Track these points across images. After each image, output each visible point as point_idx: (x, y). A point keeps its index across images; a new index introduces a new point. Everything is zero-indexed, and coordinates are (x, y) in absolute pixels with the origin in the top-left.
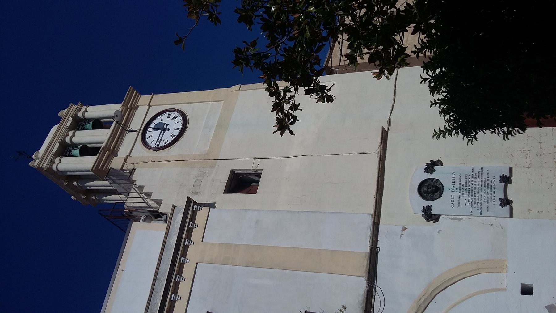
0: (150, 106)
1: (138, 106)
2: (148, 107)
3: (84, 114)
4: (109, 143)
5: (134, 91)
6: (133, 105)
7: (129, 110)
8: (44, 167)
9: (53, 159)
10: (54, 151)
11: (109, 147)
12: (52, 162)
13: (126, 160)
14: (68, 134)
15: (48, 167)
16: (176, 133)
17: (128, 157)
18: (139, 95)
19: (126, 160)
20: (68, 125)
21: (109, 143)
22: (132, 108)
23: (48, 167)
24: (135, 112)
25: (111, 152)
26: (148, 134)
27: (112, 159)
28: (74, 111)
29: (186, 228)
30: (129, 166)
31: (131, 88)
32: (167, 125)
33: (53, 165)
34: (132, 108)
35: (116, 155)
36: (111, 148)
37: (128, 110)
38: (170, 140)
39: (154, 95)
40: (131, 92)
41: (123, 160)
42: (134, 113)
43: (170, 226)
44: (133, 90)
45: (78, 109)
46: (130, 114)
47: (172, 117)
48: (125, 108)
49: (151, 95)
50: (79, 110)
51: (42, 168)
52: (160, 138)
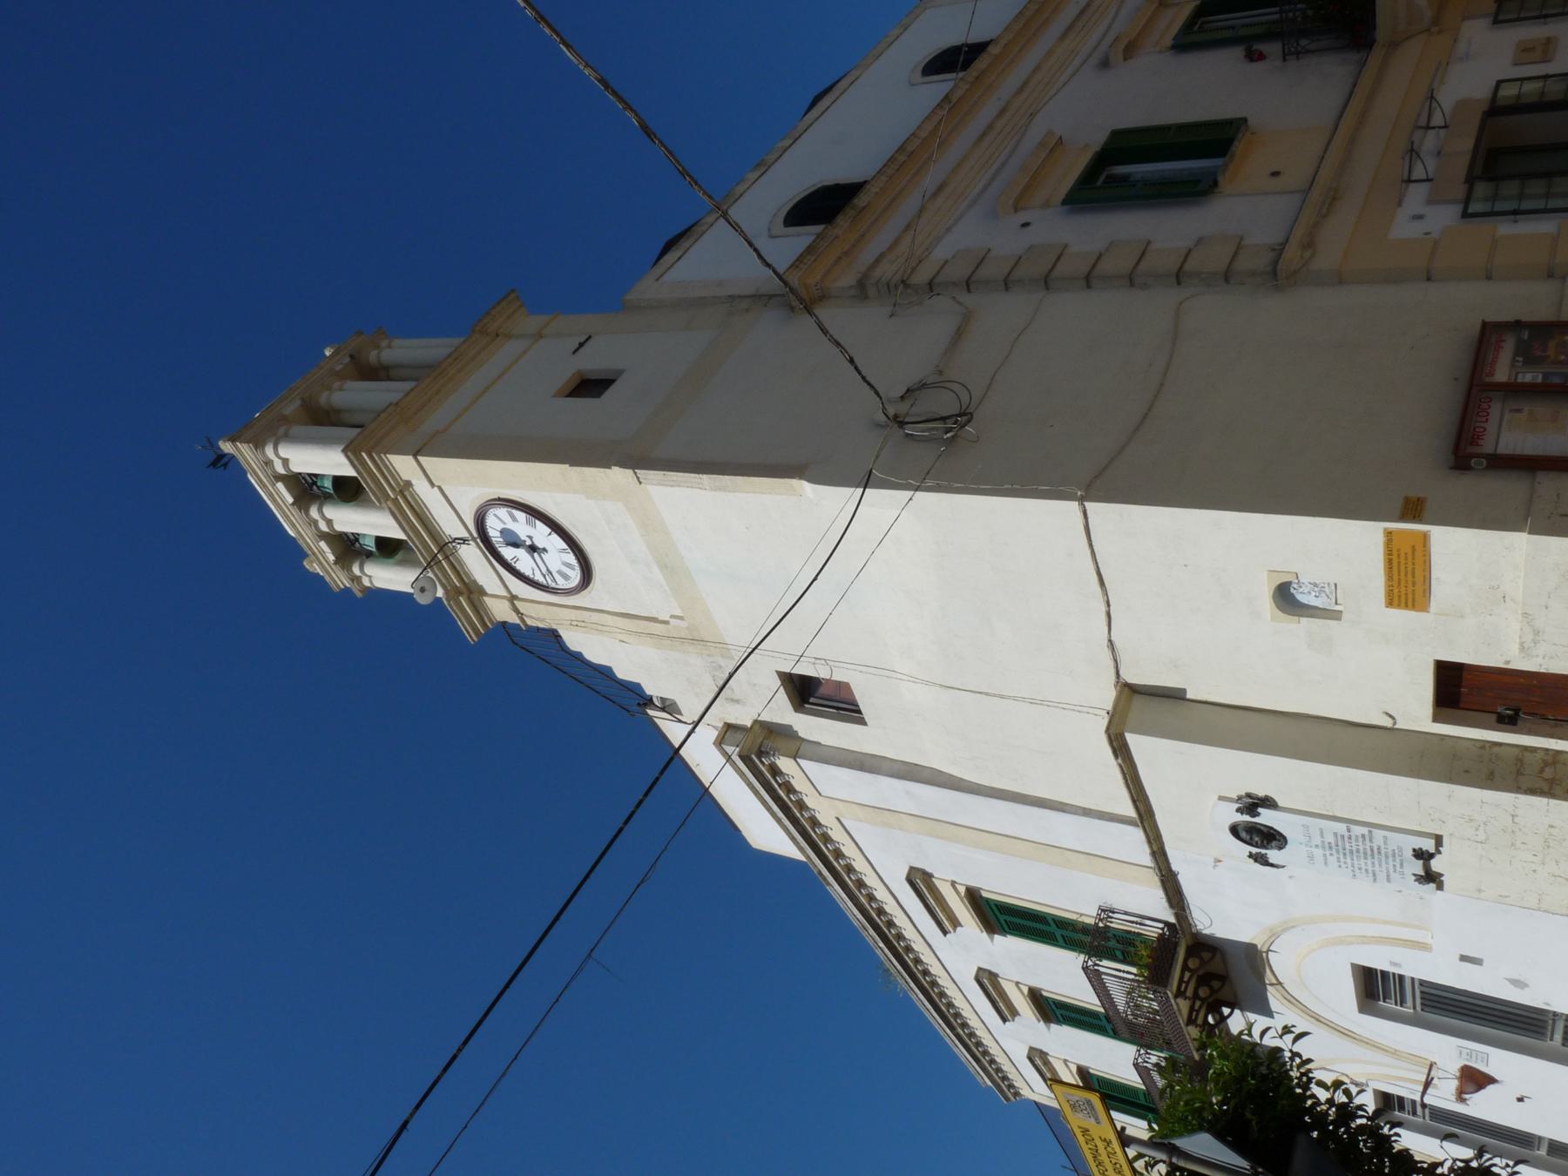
4: (444, 581)
5: (362, 456)
6: (394, 485)
7: (399, 497)
11: (450, 585)
21: (444, 581)
22: (401, 492)
25: (464, 590)
27: (482, 604)
29: (776, 786)
33: (361, 583)
34: (401, 492)
35: (481, 592)
36: (458, 585)
37: (398, 501)
45: (266, 464)
46: (413, 504)
50: (269, 463)
51: (347, 591)
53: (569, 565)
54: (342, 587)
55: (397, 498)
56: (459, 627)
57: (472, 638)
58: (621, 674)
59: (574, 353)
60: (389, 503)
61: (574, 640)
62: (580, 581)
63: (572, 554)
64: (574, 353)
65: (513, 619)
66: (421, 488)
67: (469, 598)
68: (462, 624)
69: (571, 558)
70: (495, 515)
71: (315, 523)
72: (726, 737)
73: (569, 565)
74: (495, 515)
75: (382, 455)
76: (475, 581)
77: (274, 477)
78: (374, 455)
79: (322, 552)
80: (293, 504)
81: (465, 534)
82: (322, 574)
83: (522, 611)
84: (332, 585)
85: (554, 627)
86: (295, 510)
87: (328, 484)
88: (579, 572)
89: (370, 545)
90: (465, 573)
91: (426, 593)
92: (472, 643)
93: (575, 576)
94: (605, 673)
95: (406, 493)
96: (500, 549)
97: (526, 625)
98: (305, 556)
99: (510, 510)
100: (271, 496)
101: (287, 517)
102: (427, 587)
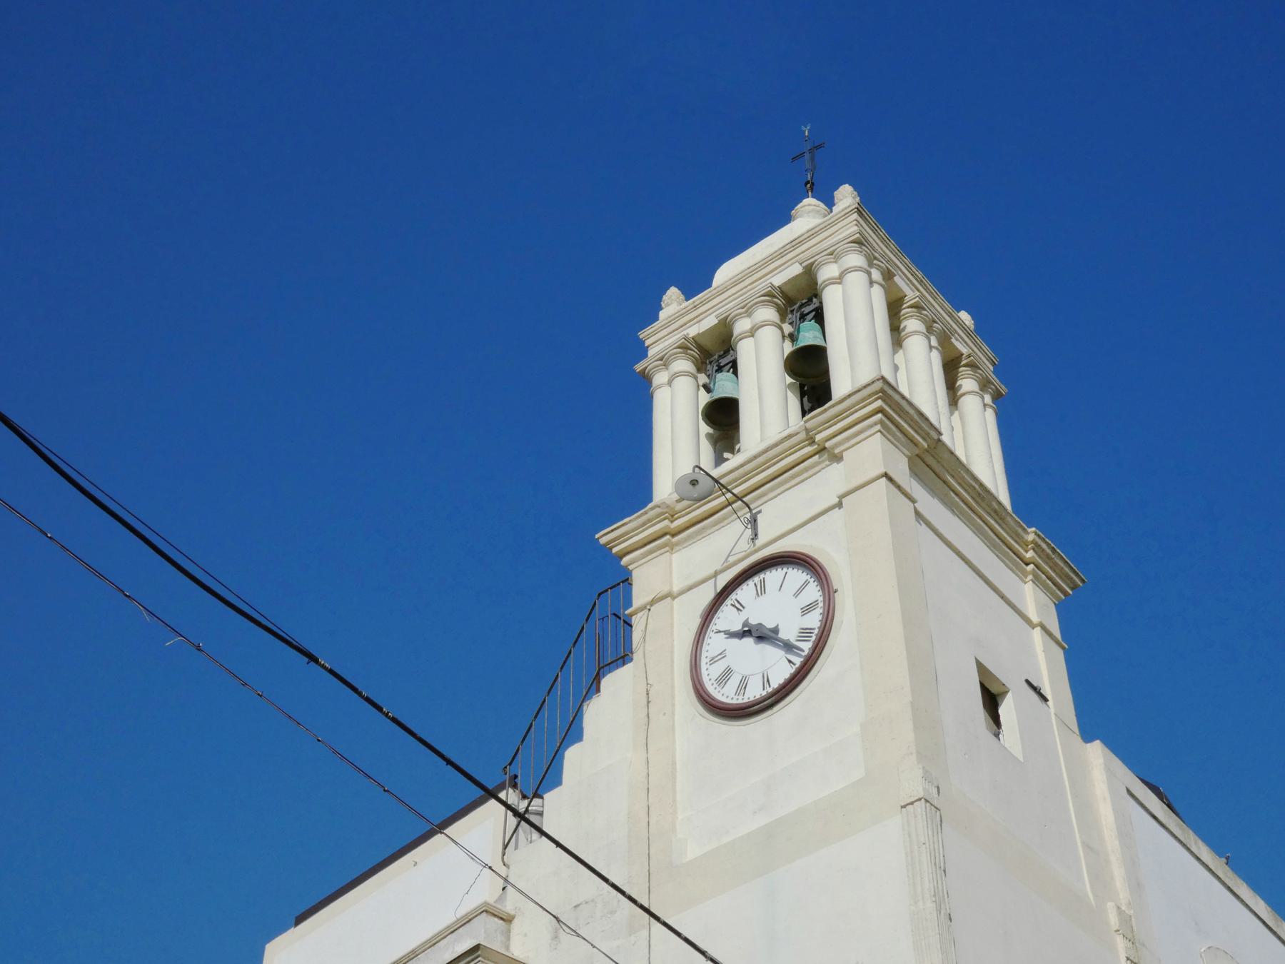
0: (840, 505)
1: (838, 458)
2: (836, 500)
3: (827, 286)
7: (816, 446)
8: (651, 352)
10: (693, 331)
12: (664, 361)
13: (653, 602)
15: (646, 368)
18: (876, 424)
19: (653, 602)
20: (778, 280)
22: (822, 450)
23: (646, 368)
28: (815, 250)
43: (445, 937)
44: (877, 393)
50: (834, 256)
51: (642, 352)
53: (743, 685)
54: (647, 343)
56: (622, 519)
57: (604, 537)
58: (572, 755)
59: (1028, 682)
61: (617, 683)
62: (714, 699)
63: (764, 693)
64: (1028, 682)
65: (640, 596)
66: (831, 480)
68: (631, 522)
69: (755, 692)
70: (806, 583)
71: (749, 313)
72: (496, 919)
73: (743, 685)
74: (806, 583)
77: (812, 264)
79: (698, 319)
80: (772, 286)
81: (763, 538)
82: (663, 315)
83: (652, 608)
84: (648, 330)
85: (637, 656)
86: (762, 286)
87: (809, 336)
88: (734, 702)
89: (724, 386)
90: (704, 529)
91: (691, 487)
92: (597, 536)
93: (727, 695)
94: (572, 731)
96: (751, 583)
97: (631, 615)
98: (689, 293)
99: (821, 605)
100: (781, 253)
101: (752, 271)
102: (697, 487)
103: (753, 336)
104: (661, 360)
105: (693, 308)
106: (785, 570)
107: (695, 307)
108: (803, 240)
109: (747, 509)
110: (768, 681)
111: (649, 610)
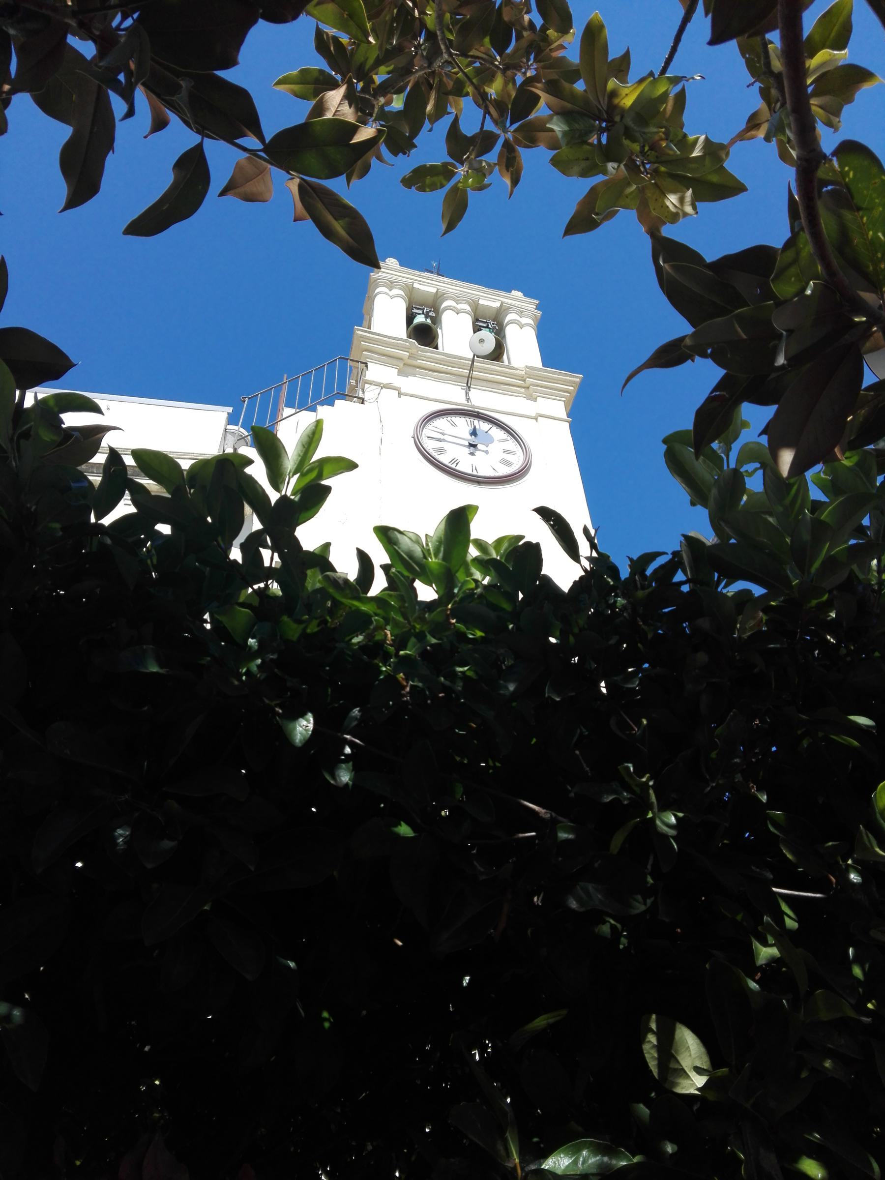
2: (534, 415)
9: (398, 285)
12: (391, 285)
14: (460, 303)
16: (464, 467)
17: (396, 390)
24: (520, 395)
26: (460, 421)
27: (392, 366)
30: (370, 393)
31: (576, 377)
32: (487, 452)
38: (445, 459)
39: (568, 423)
40: (565, 379)
41: (385, 382)
42: (516, 394)
44: (574, 382)
47: (508, 457)
48: (523, 373)
49: (565, 416)
50: (521, 313)
52: (445, 437)
55: (524, 381)
60: (523, 373)
67: (401, 359)
74: (506, 440)
75: (565, 399)
76: (414, 375)
78: (569, 395)
88: (450, 465)
95: (523, 390)
102: (484, 345)
103: (457, 314)
104: (391, 283)
105: (418, 275)
106: (490, 426)
107: (420, 275)
108: (500, 295)
109: (465, 385)
110: (476, 469)
111: (382, 388)
